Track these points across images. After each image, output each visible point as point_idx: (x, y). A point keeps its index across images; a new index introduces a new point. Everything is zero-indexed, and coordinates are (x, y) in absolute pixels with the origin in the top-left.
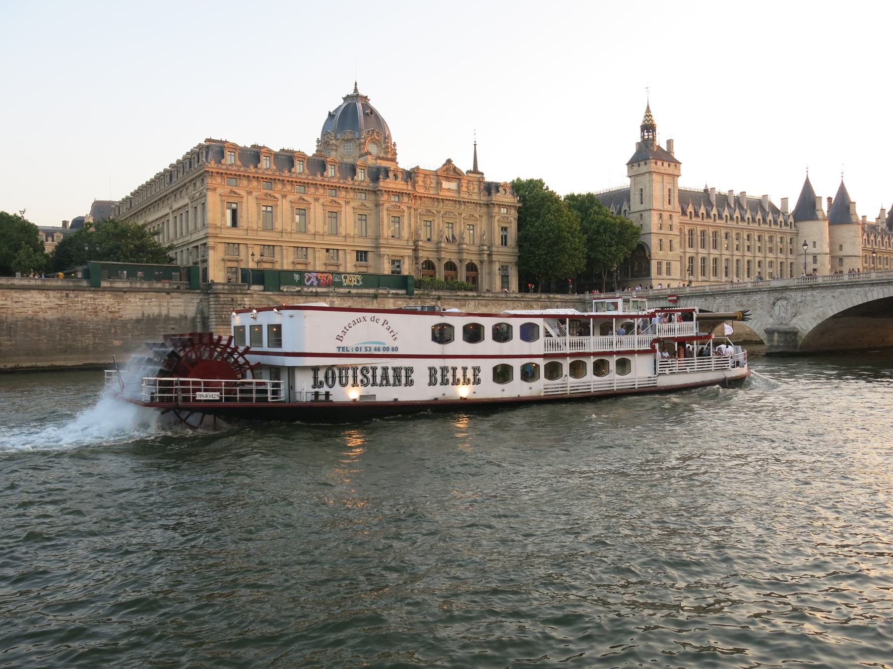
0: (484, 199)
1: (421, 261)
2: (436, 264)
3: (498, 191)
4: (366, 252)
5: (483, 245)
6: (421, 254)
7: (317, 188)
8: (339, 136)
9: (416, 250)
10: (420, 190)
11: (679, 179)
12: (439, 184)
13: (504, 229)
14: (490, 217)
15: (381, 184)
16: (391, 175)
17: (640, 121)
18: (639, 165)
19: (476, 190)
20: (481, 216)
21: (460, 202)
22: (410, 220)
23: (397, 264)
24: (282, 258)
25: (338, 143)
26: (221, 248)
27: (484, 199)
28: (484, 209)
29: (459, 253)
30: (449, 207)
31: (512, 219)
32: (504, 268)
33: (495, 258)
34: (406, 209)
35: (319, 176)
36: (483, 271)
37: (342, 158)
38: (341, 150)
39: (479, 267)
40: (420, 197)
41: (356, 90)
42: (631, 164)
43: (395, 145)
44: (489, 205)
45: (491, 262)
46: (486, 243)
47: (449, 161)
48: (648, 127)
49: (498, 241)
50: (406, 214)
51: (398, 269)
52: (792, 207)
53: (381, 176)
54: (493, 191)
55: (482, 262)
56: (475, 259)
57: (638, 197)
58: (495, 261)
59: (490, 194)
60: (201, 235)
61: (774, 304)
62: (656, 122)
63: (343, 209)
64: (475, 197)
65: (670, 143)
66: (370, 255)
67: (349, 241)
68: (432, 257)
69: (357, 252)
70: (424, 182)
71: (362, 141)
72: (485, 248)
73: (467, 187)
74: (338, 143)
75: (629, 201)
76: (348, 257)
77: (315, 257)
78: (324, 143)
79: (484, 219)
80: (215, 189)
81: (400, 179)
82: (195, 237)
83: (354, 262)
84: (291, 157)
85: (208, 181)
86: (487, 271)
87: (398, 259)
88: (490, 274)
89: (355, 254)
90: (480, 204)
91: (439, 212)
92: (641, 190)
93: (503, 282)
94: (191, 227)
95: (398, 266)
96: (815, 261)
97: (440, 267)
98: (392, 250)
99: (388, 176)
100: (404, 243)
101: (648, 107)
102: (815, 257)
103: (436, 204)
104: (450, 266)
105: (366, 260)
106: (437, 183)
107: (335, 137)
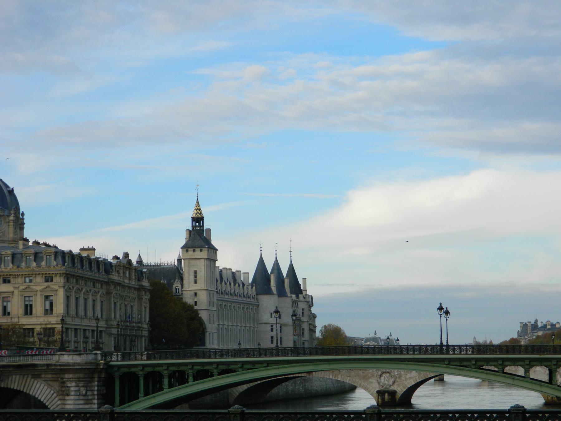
11: (217, 262)
14: (140, 299)
15: (111, 276)
17: (191, 213)
18: (194, 251)
19: (134, 278)
42: (185, 248)
48: (198, 220)
52: (250, 281)
57: (192, 277)
61: (381, 376)
62: (204, 216)
64: (133, 283)
65: (209, 230)
75: (182, 279)
92: (195, 272)
96: (272, 330)
101: (198, 201)
102: (272, 326)
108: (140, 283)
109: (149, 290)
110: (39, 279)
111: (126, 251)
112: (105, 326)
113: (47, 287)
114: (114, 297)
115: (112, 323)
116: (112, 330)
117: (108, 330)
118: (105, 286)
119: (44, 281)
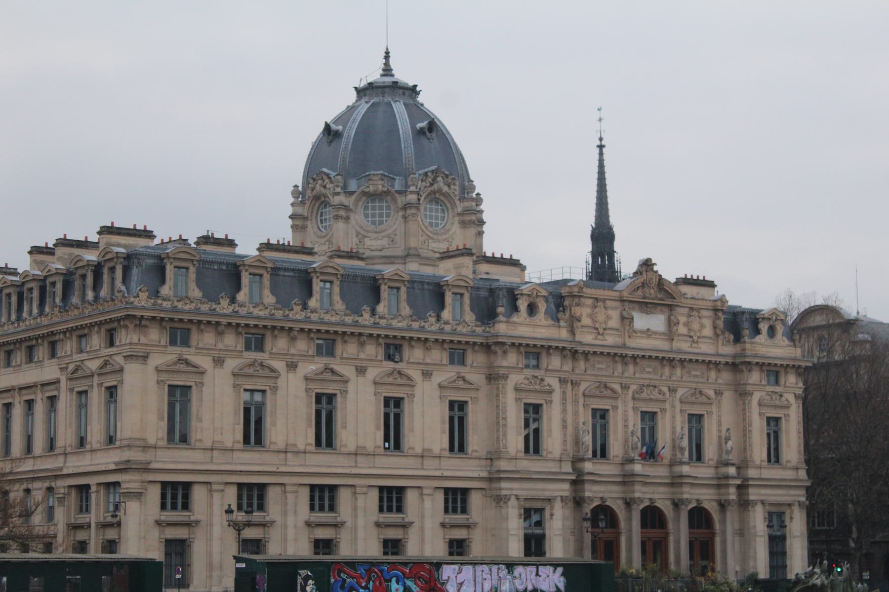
0: (728, 350)
1: (588, 509)
2: (621, 515)
3: (758, 332)
4: (465, 492)
5: (727, 464)
6: (591, 491)
7: (362, 344)
8: (353, 185)
9: (577, 483)
10: (587, 338)
12: (626, 320)
13: (774, 423)
14: (742, 394)
15: (501, 328)
16: (522, 304)
19: (708, 331)
20: (718, 393)
21: (671, 360)
22: (564, 411)
23: (535, 518)
24: (285, 513)
25: (349, 201)
26: (154, 494)
27: (728, 350)
28: (726, 376)
29: (672, 485)
30: (646, 374)
31: (791, 398)
32: (777, 519)
33: (753, 494)
34: (554, 382)
35: (366, 316)
36: (726, 528)
37: (361, 237)
38: (358, 218)
39: (716, 517)
40: (586, 354)
41: (387, 71)
43: (478, 200)
44: (736, 366)
45: (744, 504)
46: (733, 457)
47: (647, 265)
49: (759, 452)
50: (556, 397)
51: (538, 531)
53: (500, 310)
54: (746, 332)
55: (723, 506)
56: (707, 498)
58: (755, 503)
59: (738, 339)
60: (108, 459)
63: (418, 391)
64: (706, 348)
66: (475, 500)
67: (431, 468)
68: (612, 496)
69: (447, 491)
70: (591, 316)
71: (412, 198)
72: (732, 471)
73: (686, 324)
74: (349, 201)
76: (428, 503)
77: (355, 509)
78: (313, 199)
79: (728, 397)
80: (145, 357)
81: (540, 316)
82: (75, 464)
83: (441, 516)
84: (306, 272)
85: (126, 337)
86: (737, 526)
87: (539, 505)
88: (742, 532)
89: (440, 497)
90: (717, 364)
91: (625, 387)
93: (772, 554)
94: (66, 437)
95: (539, 524)
97: (629, 519)
98: (526, 485)
99: (516, 309)
100: (553, 467)
103: (619, 367)
104: (652, 517)
105: (464, 511)
106: (623, 318)
107: (345, 187)
108: (738, 348)
109: (797, 369)
110: (96, 341)
111: (645, 257)
112: (484, 474)
113: (106, 363)
114: (517, 389)
115: (503, 465)
116: (504, 485)
117: (494, 485)
118: (476, 359)
119: (103, 345)
